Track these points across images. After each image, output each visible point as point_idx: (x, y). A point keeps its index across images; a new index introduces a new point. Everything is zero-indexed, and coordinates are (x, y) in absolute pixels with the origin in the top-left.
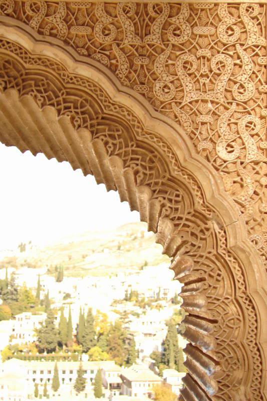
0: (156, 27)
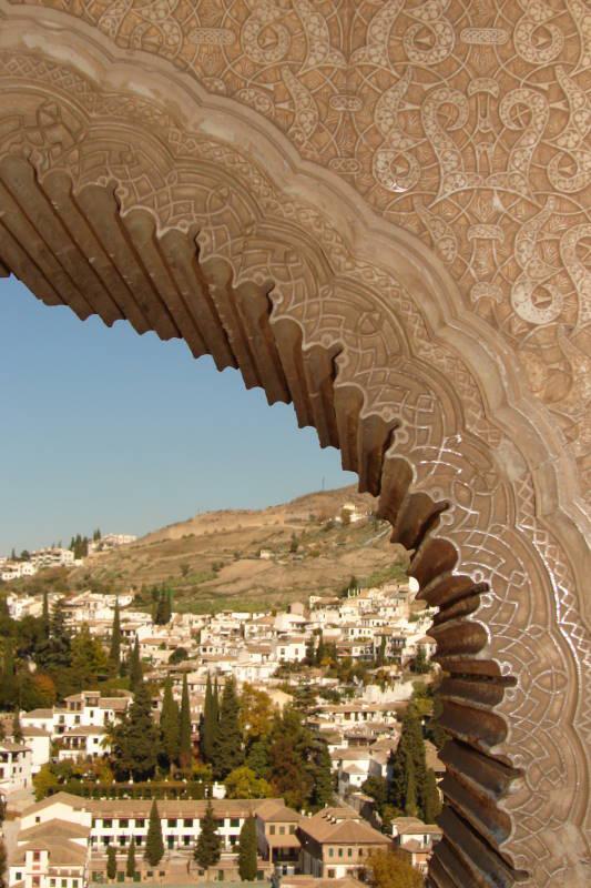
0: (378, 31)
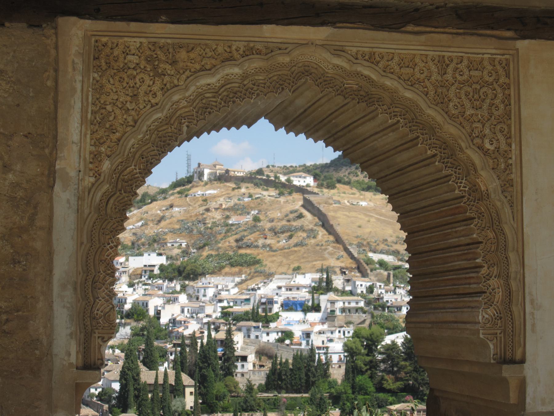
0: (450, 70)
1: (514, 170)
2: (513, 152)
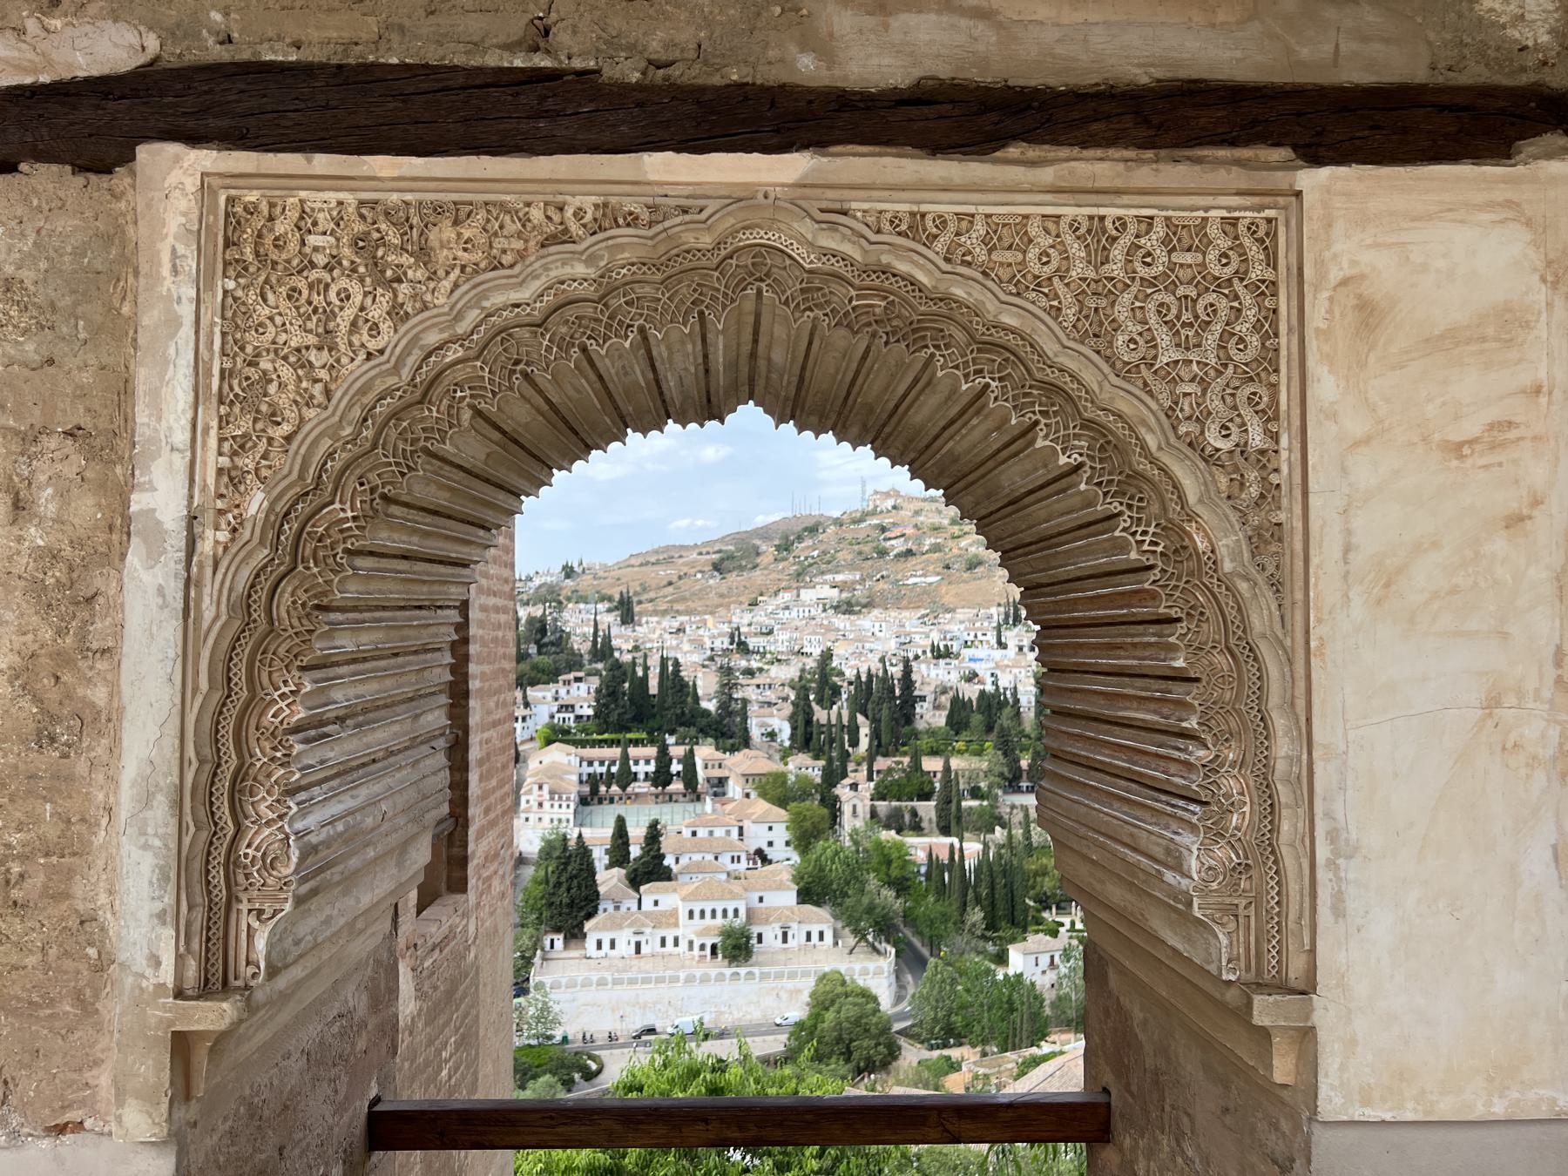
0: (1117, 252)
1: (1285, 502)
2: (1284, 455)
